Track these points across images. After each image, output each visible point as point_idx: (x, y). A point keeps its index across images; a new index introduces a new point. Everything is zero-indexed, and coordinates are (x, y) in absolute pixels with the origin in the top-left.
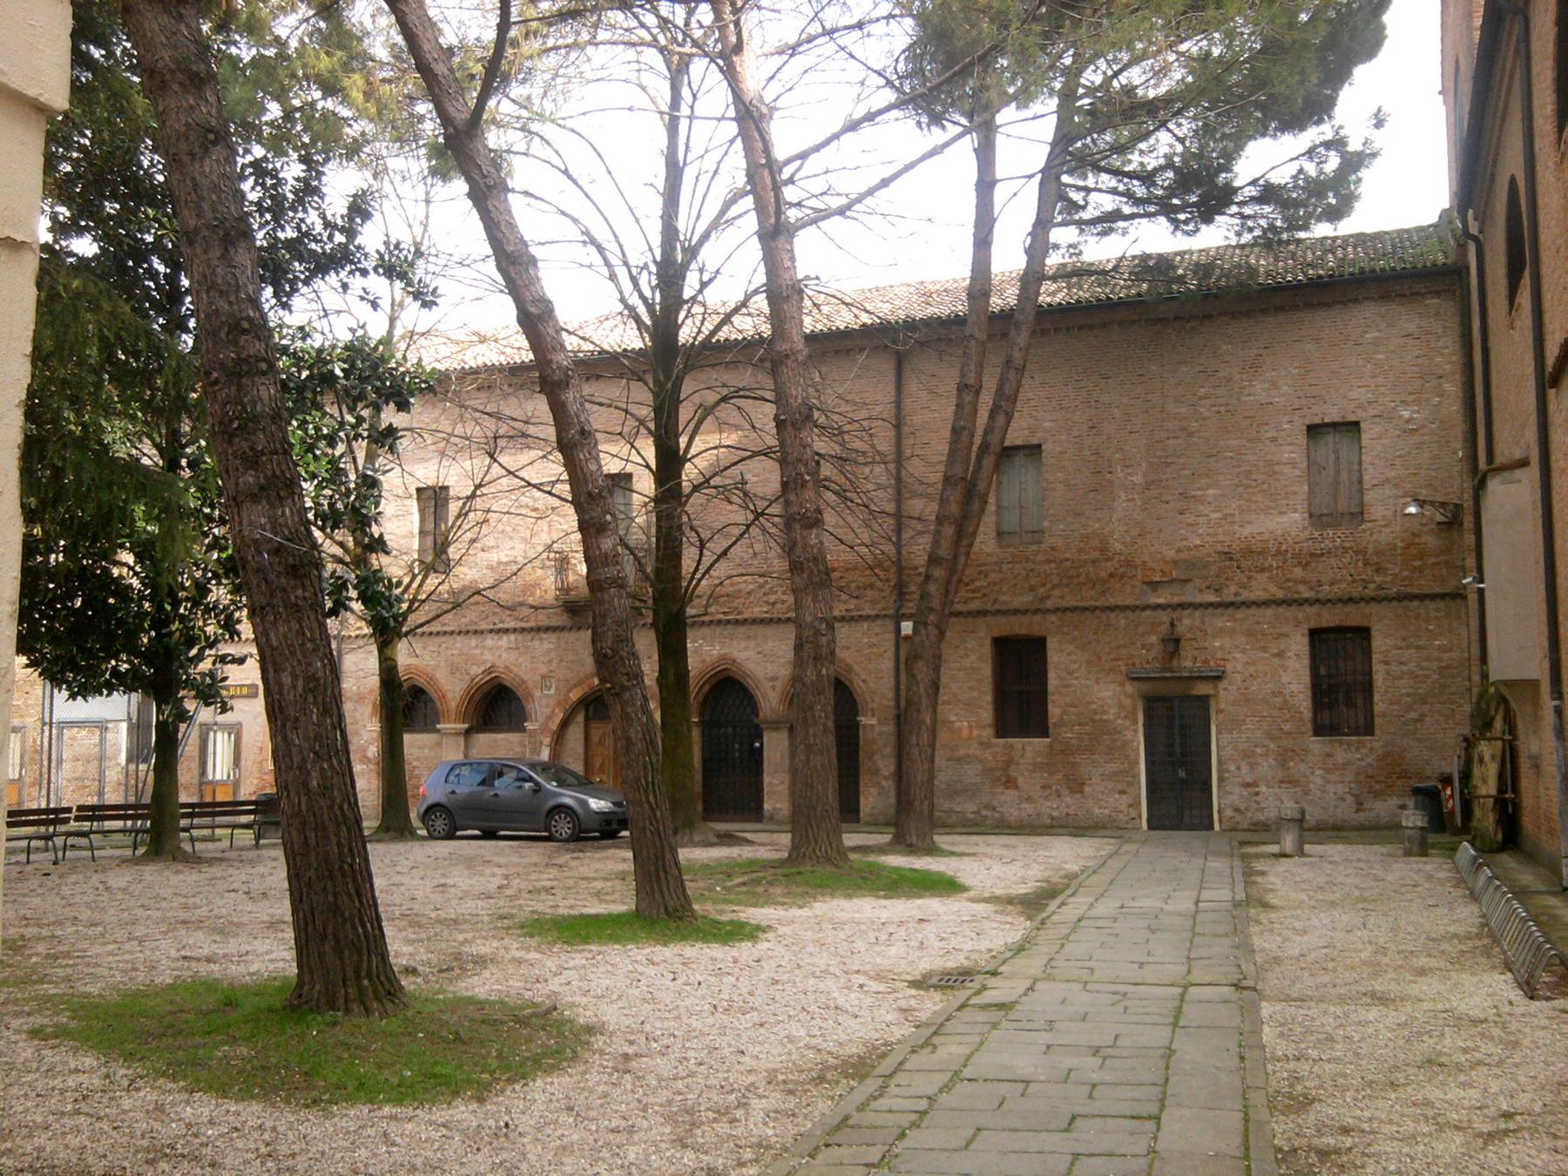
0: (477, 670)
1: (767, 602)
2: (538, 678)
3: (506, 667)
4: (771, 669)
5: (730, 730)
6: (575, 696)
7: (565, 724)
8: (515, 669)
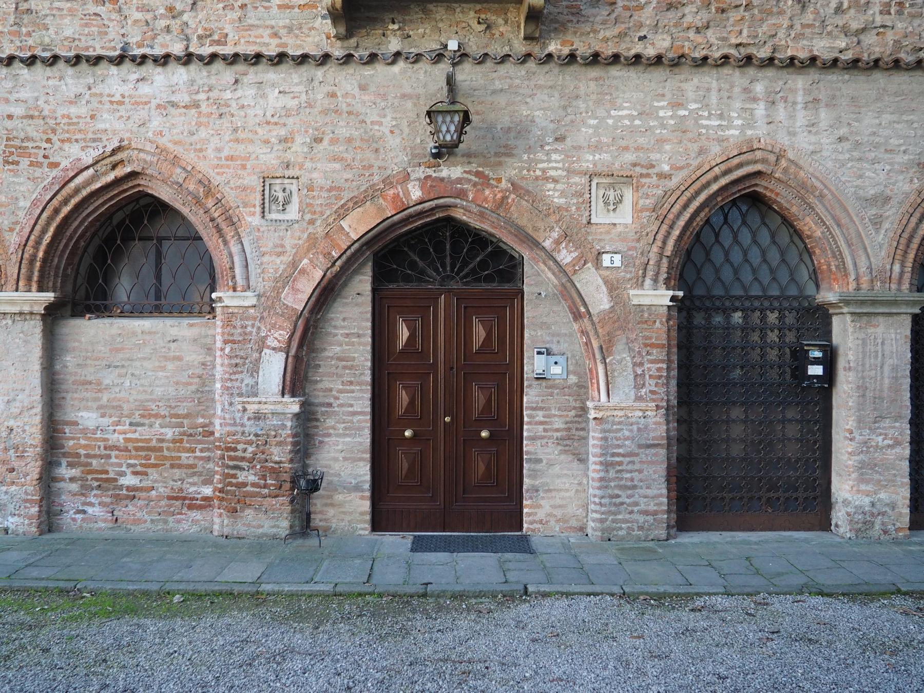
0: (75, 154)
1: (845, 31)
2: (254, 181)
3: (161, 151)
4: (874, 179)
5: (737, 317)
6: (357, 225)
7: (327, 294)
8: (190, 158)
